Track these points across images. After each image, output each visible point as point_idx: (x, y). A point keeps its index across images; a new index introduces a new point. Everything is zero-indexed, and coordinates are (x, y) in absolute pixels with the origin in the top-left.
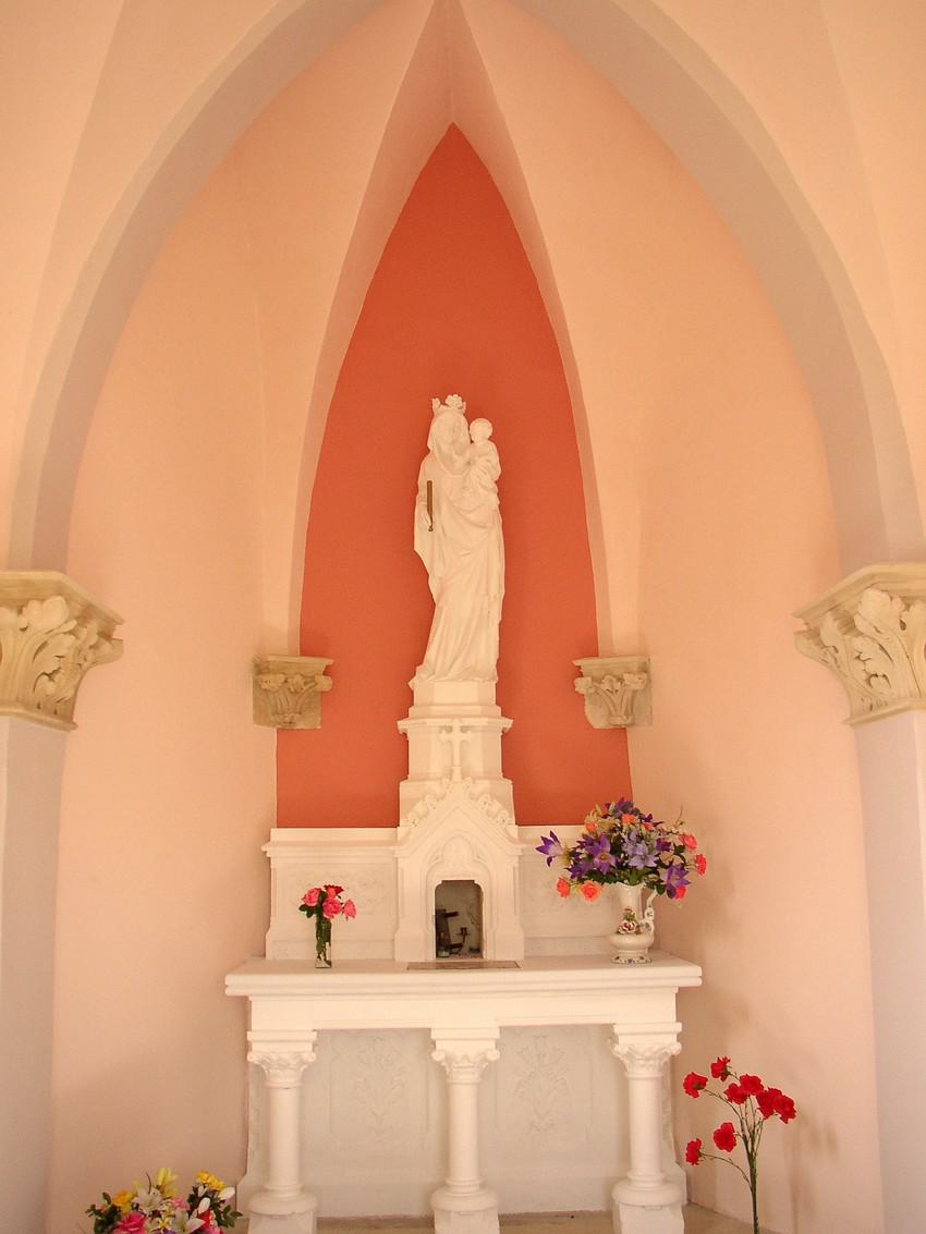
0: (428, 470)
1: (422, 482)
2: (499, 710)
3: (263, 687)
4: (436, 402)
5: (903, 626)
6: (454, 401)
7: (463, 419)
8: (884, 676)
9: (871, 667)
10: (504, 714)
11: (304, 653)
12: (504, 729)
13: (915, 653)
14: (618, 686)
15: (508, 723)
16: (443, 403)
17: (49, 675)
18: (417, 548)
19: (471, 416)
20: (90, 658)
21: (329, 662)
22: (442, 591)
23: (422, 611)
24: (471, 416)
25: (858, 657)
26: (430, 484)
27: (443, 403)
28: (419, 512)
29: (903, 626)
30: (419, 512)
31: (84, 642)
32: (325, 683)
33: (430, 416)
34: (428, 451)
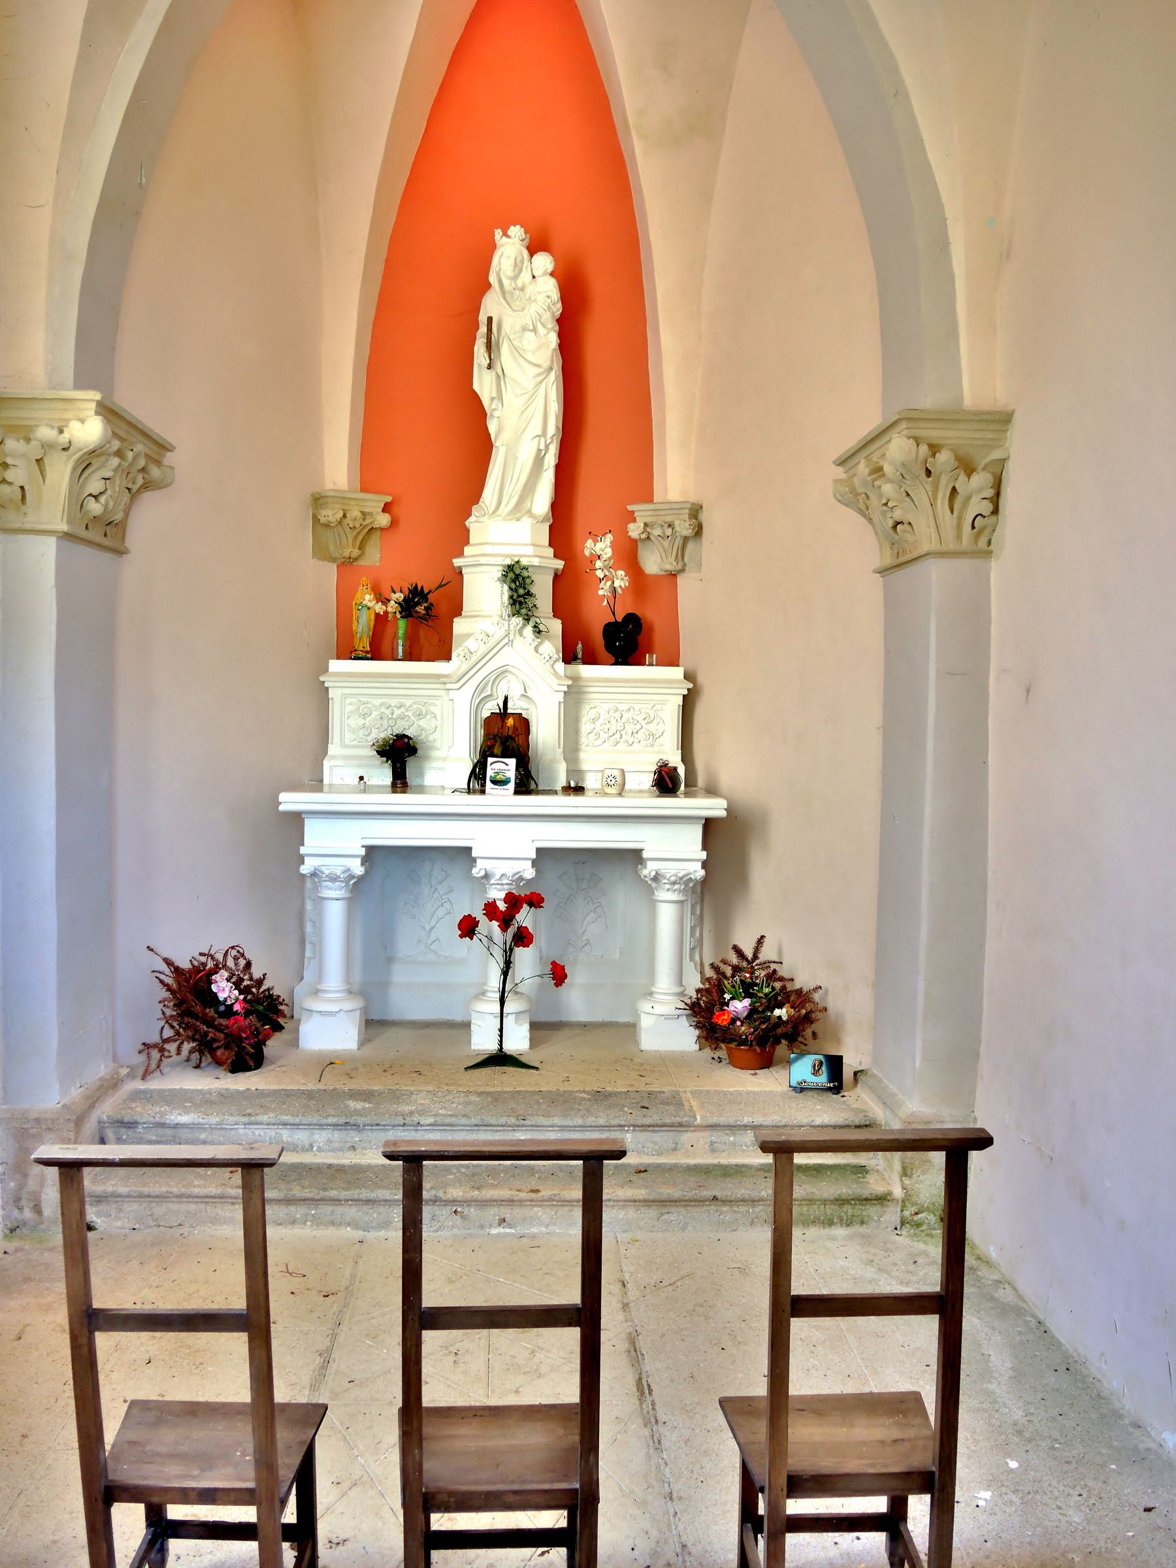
0: (491, 305)
1: (483, 318)
2: (551, 551)
3: (322, 521)
4: (498, 233)
5: (929, 473)
6: (516, 231)
7: (525, 253)
8: (910, 523)
9: (898, 515)
10: (556, 556)
11: (364, 489)
12: (557, 569)
13: (939, 501)
14: (669, 532)
15: (559, 564)
16: (505, 234)
17: (95, 497)
18: (476, 387)
19: (533, 250)
20: (140, 481)
21: (389, 499)
22: (499, 431)
23: (482, 448)
24: (533, 250)
25: (886, 504)
26: (490, 320)
27: (505, 234)
28: (478, 350)
29: (929, 473)
30: (478, 350)
31: (130, 465)
32: (384, 520)
33: (492, 247)
34: (489, 286)
